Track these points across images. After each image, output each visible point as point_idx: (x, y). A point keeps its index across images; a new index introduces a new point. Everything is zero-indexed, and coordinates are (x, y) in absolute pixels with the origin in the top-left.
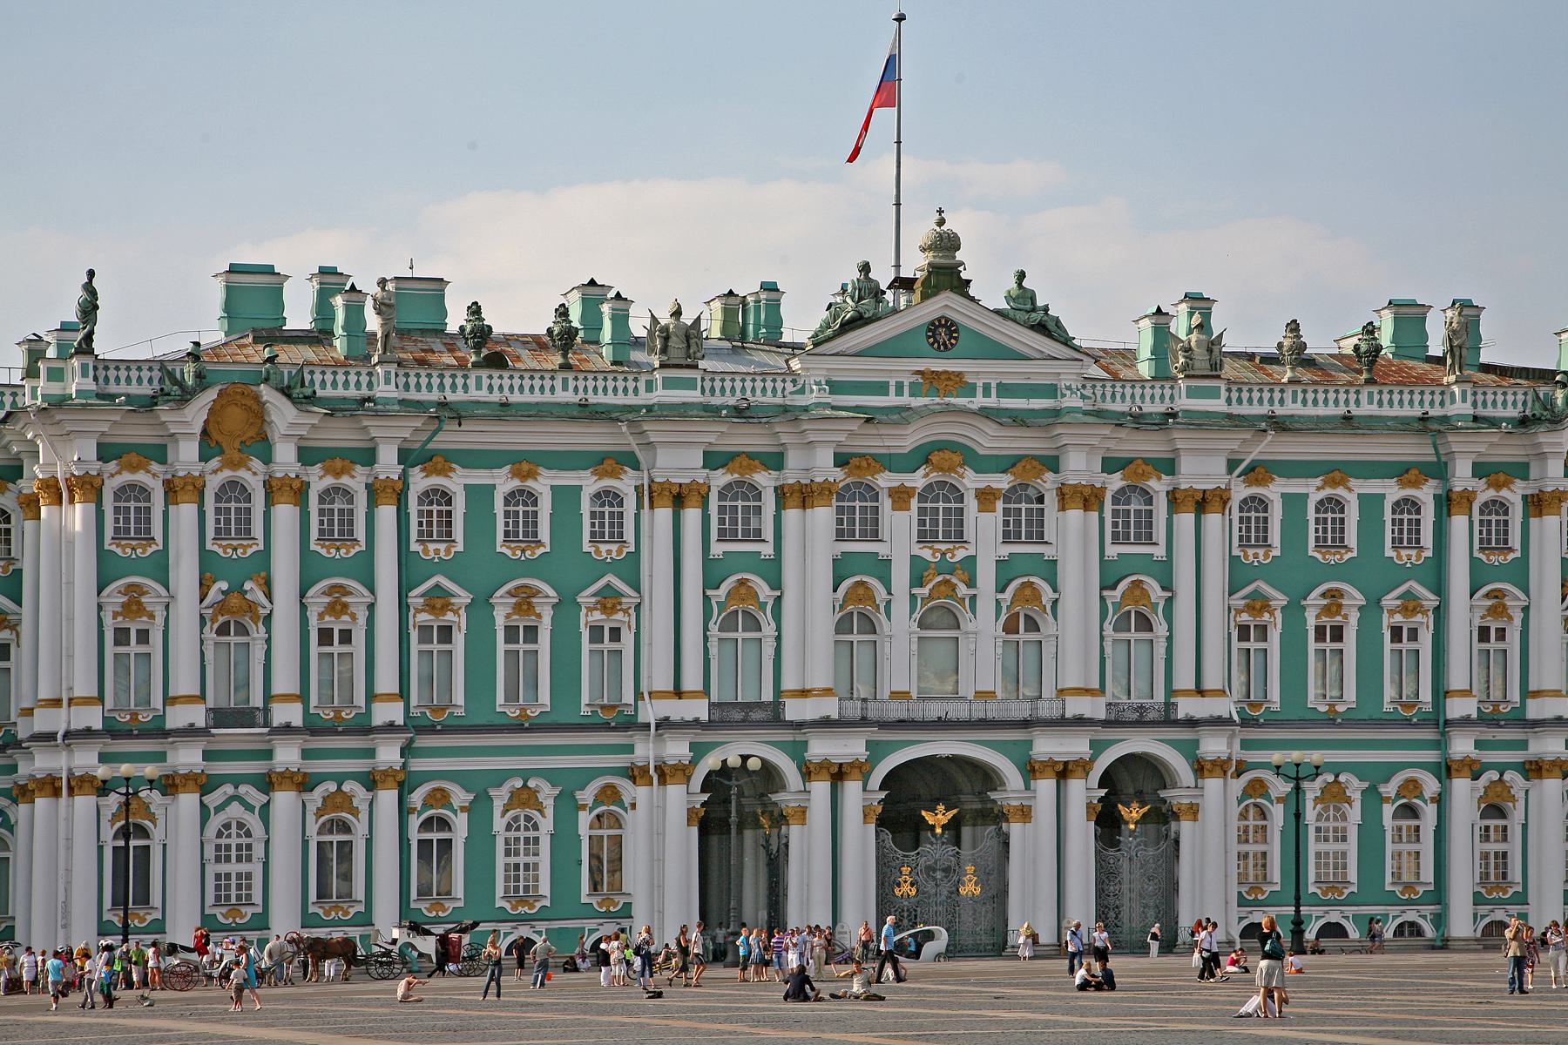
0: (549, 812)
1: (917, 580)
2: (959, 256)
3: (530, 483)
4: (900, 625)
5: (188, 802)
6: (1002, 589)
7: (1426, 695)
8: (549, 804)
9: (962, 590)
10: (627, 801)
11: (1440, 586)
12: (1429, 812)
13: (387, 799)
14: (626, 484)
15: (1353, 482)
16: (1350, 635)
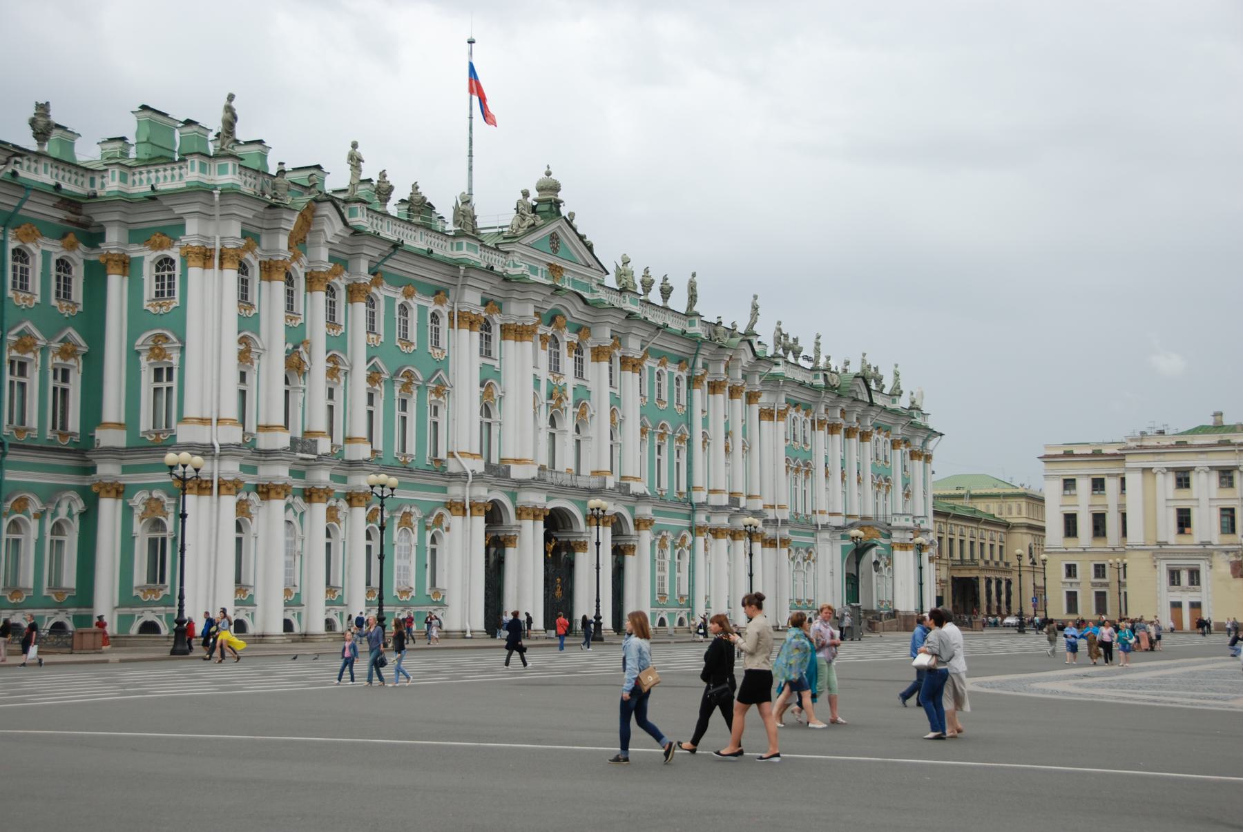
0: (416, 530)
1: (551, 396)
2: (561, 196)
3: (409, 301)
4: (544, 421)
5: (278, 505)
6: (576, 406)
7: (683, 488)
8: (415, 523)
9: (565, 404)
10: (445, 525)
11: (690, 425)
12: (687, 552)
13: (361, 513)
14: (444, 310)
15: (668, 364)
16: (665, 450)
